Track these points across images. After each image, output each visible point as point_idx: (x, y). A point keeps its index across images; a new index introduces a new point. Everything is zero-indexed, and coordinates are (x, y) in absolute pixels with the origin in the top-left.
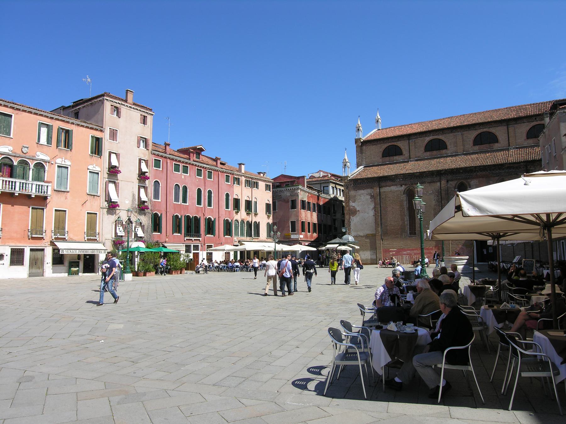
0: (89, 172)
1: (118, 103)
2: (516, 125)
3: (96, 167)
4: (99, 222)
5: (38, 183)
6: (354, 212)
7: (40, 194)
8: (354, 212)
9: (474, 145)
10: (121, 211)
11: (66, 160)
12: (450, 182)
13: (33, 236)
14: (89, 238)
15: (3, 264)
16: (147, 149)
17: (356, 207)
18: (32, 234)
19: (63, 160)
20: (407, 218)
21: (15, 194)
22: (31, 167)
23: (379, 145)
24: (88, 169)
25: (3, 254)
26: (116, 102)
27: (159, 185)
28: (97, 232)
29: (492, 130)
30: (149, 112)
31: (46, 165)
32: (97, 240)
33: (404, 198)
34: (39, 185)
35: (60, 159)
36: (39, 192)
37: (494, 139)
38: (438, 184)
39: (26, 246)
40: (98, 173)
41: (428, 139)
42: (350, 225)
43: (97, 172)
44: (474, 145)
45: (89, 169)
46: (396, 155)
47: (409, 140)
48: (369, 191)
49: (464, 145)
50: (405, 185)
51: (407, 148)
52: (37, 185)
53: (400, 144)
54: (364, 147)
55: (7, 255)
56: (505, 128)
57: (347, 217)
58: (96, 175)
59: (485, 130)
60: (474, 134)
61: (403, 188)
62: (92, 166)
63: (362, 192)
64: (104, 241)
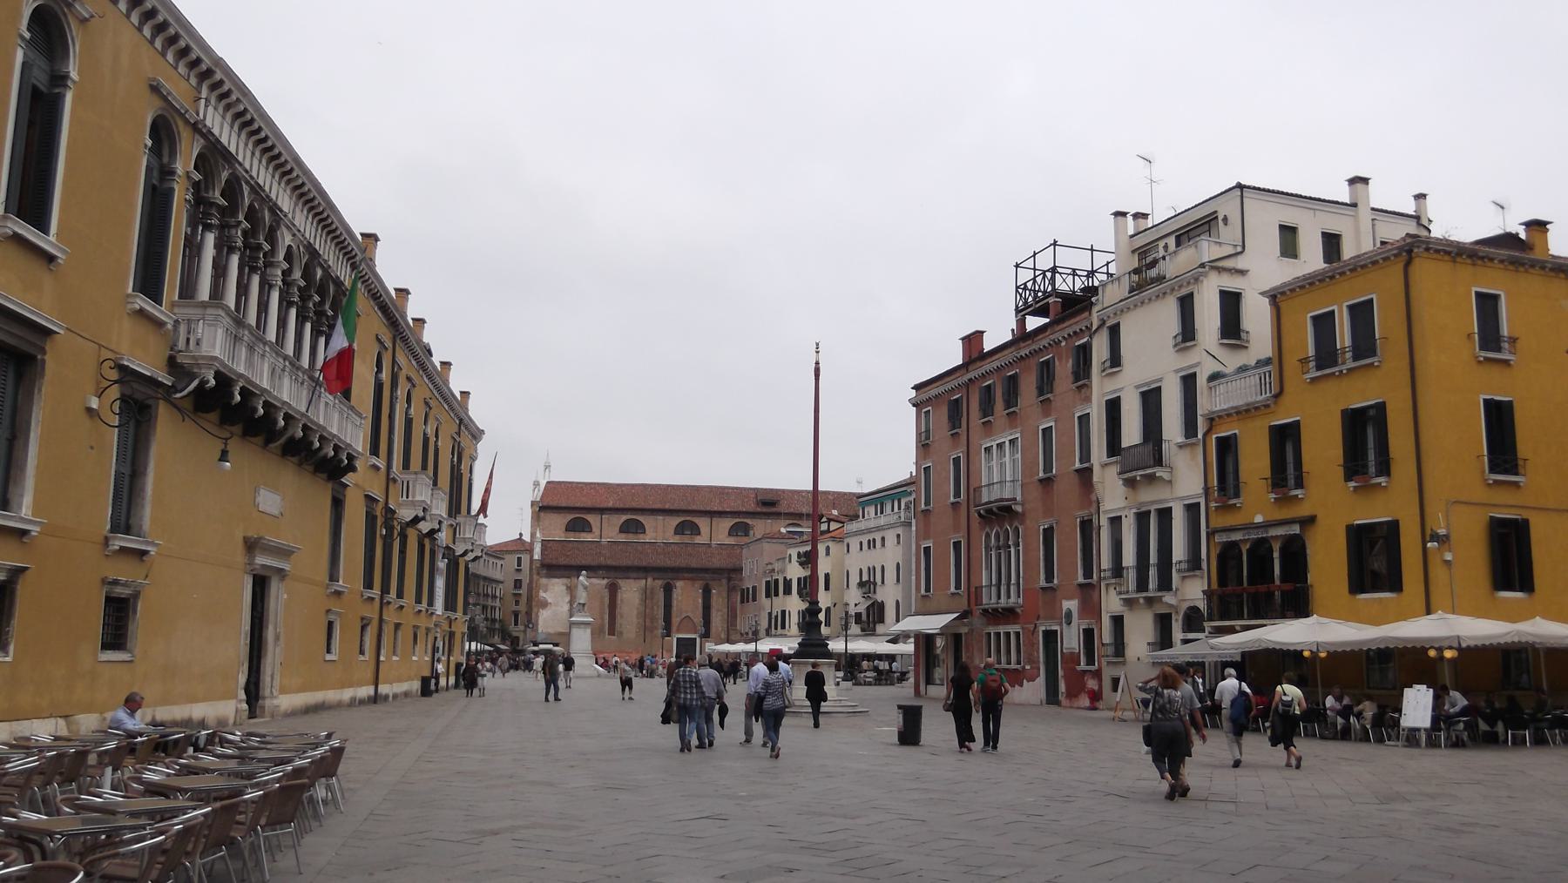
2: (720, 519)
6: (545, 604)
8: (545, 604)
9: (675, 534)
12: (657, 581)
17: (547, 598)
20: (607, 617)
23: (562, 515)
29: (696, 520)
33: (606, 594)
37: (696, 530)
38: (644, 581)
41: (624, 518)
42: (537, 621)
44: (675, 534)
46: (583, 531)
47: (602, 515)
48: (565, 580)
49: (664, 532)
50: (608, 578)
51: (599, 524)
53: (591, 518)
54: (542, 514)
56: (709, 520)
57: (535, 610)
59: (688, 518)
60: (675, 521)
61: (605, 582)
63: (557, 580)
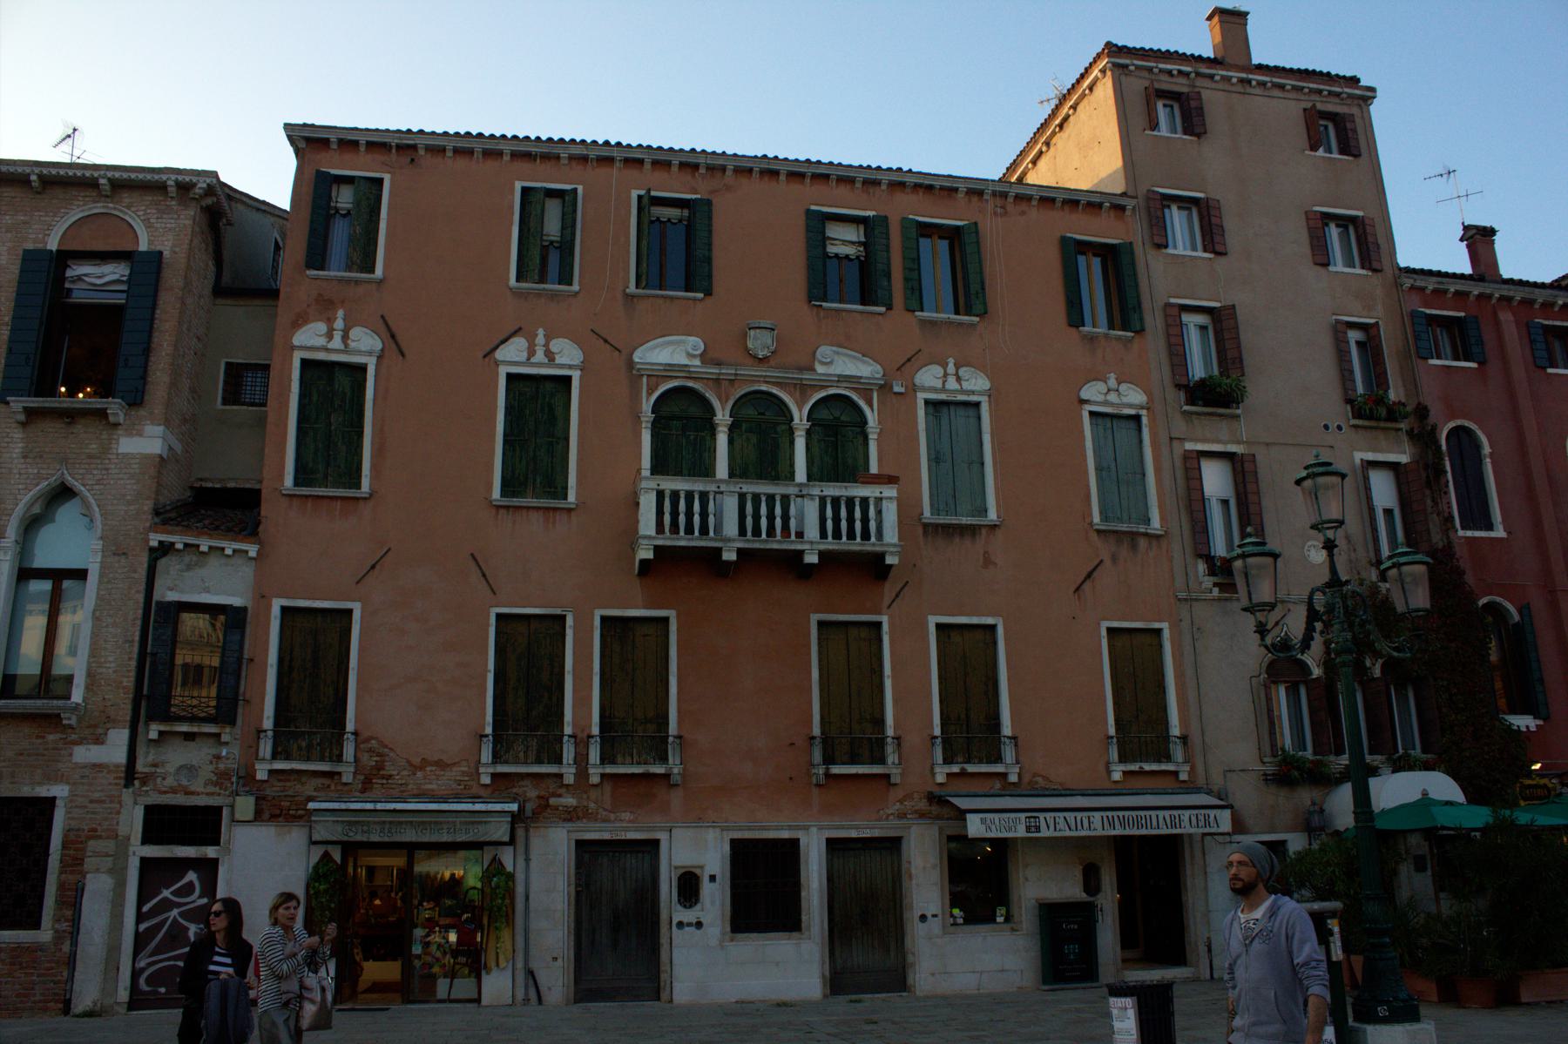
0: (1086, 415)
1: (1180, 72)
3: (1123, 387)
4: (1180, 676)
5: (832, 490)
7: (844, 545)
10: (1291, 606)
11: (962, 372)
13: (836, 770)
14: (1134, 767)
15: (699, 925)
16: (1375, 271)
18: (829, 760)
19: (951, 368)
21: (721, 556)
22: (796, 420)
24: (1083, 402)
25: (697, 871)
26: (1170, 73)
27: (1477, 447)
28: (1175, 730)
30: (1346, 90)
31: (871, 405)
32: (1183, 777)
34: (836, 501)
35: (937, 370)
36: (837, 535)
39: (806, 828)
40: (1137, 419)
43: (1132, 412)
45: (1086, 402)
52: (823, 500)
55: (713, 878)
58: (1124, 433)
62: (1101, 387)
64: (1217, 781)
